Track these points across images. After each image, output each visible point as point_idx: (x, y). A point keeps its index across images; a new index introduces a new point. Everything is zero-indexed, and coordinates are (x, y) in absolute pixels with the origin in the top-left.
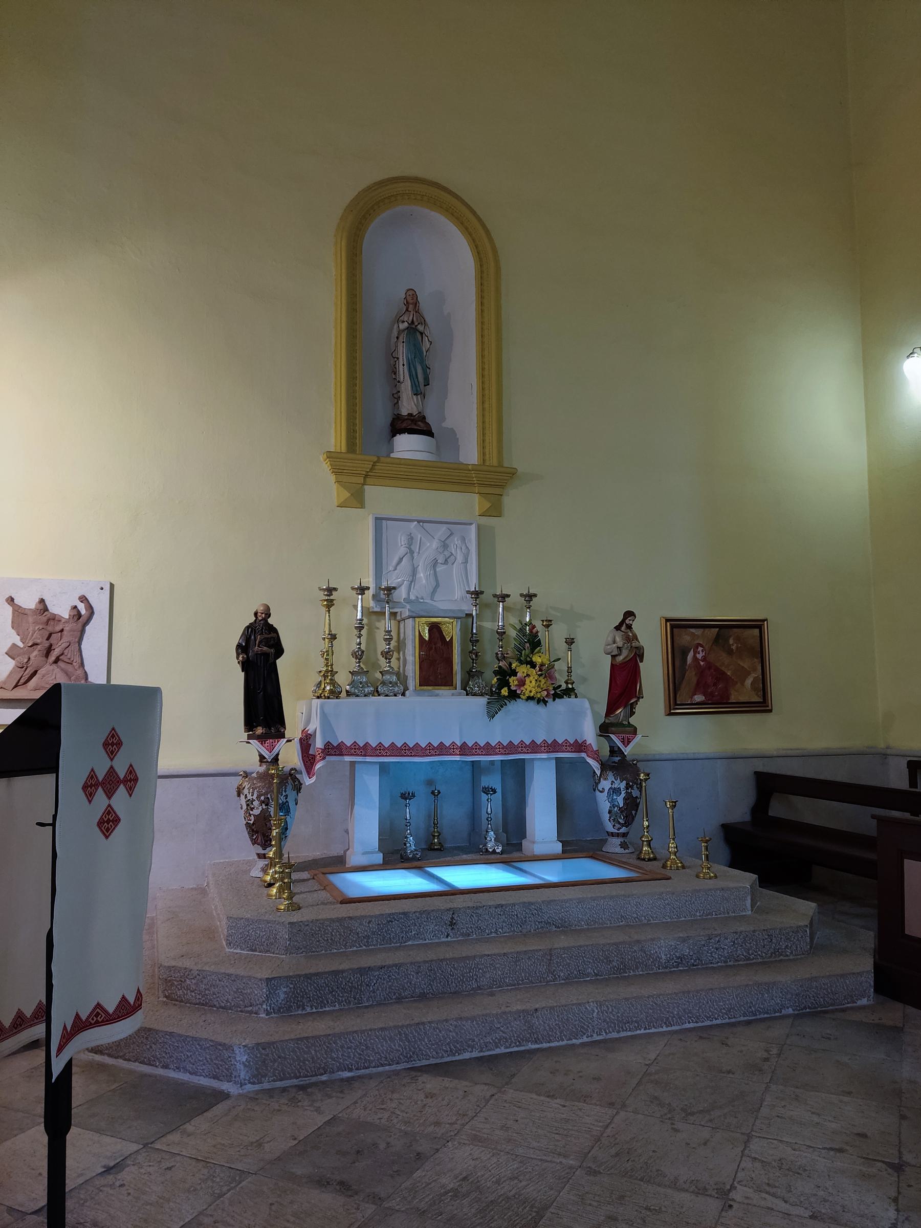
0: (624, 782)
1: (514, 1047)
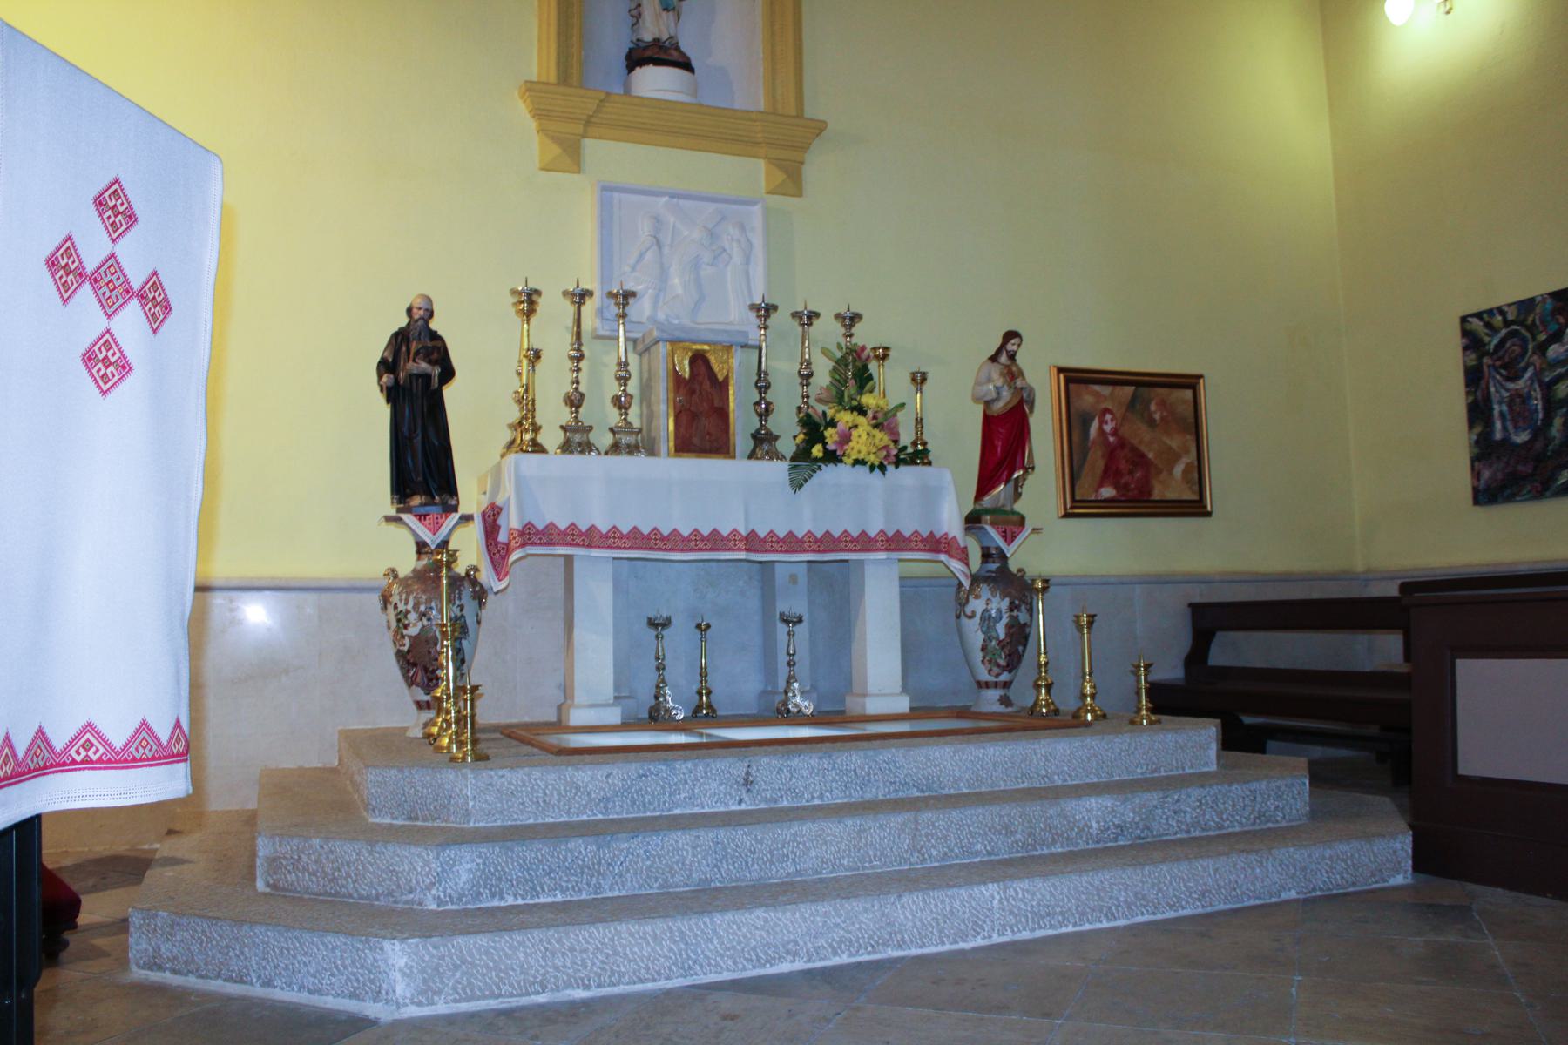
1: (863, 954)
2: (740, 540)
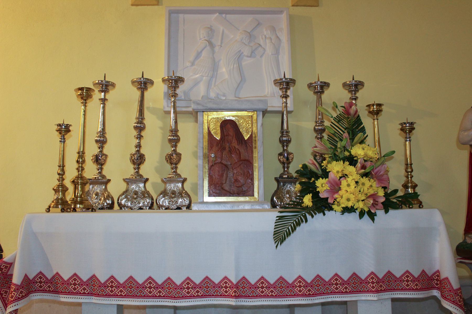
2: (231, 288)
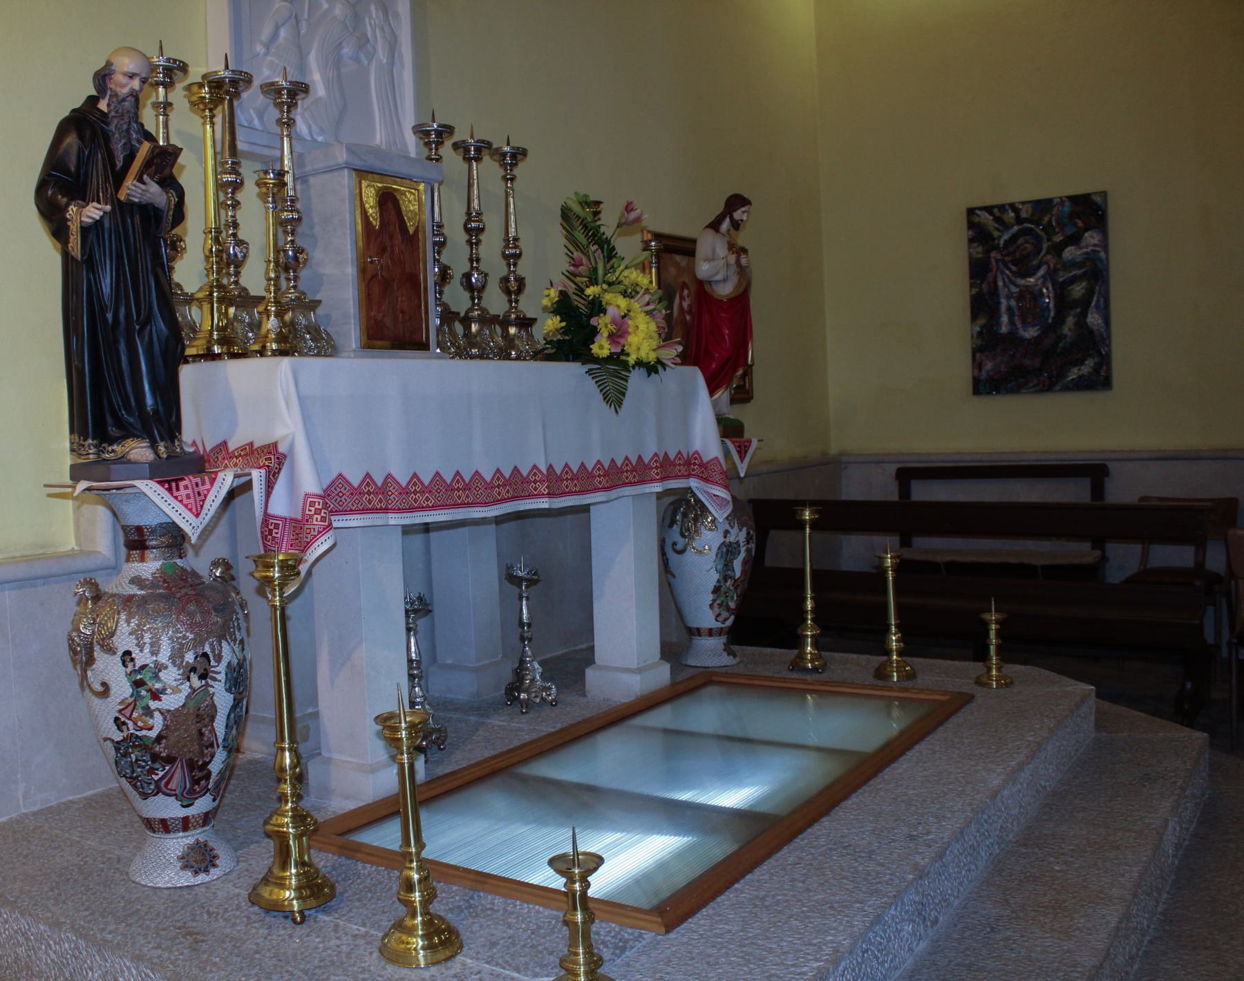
0: (744, 530)
2: (542, 481)
